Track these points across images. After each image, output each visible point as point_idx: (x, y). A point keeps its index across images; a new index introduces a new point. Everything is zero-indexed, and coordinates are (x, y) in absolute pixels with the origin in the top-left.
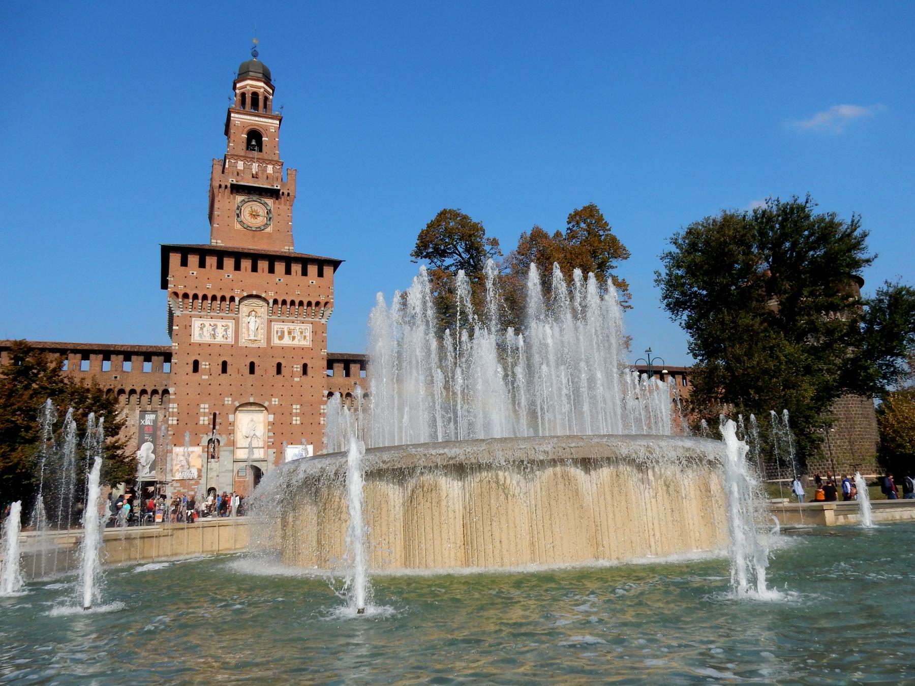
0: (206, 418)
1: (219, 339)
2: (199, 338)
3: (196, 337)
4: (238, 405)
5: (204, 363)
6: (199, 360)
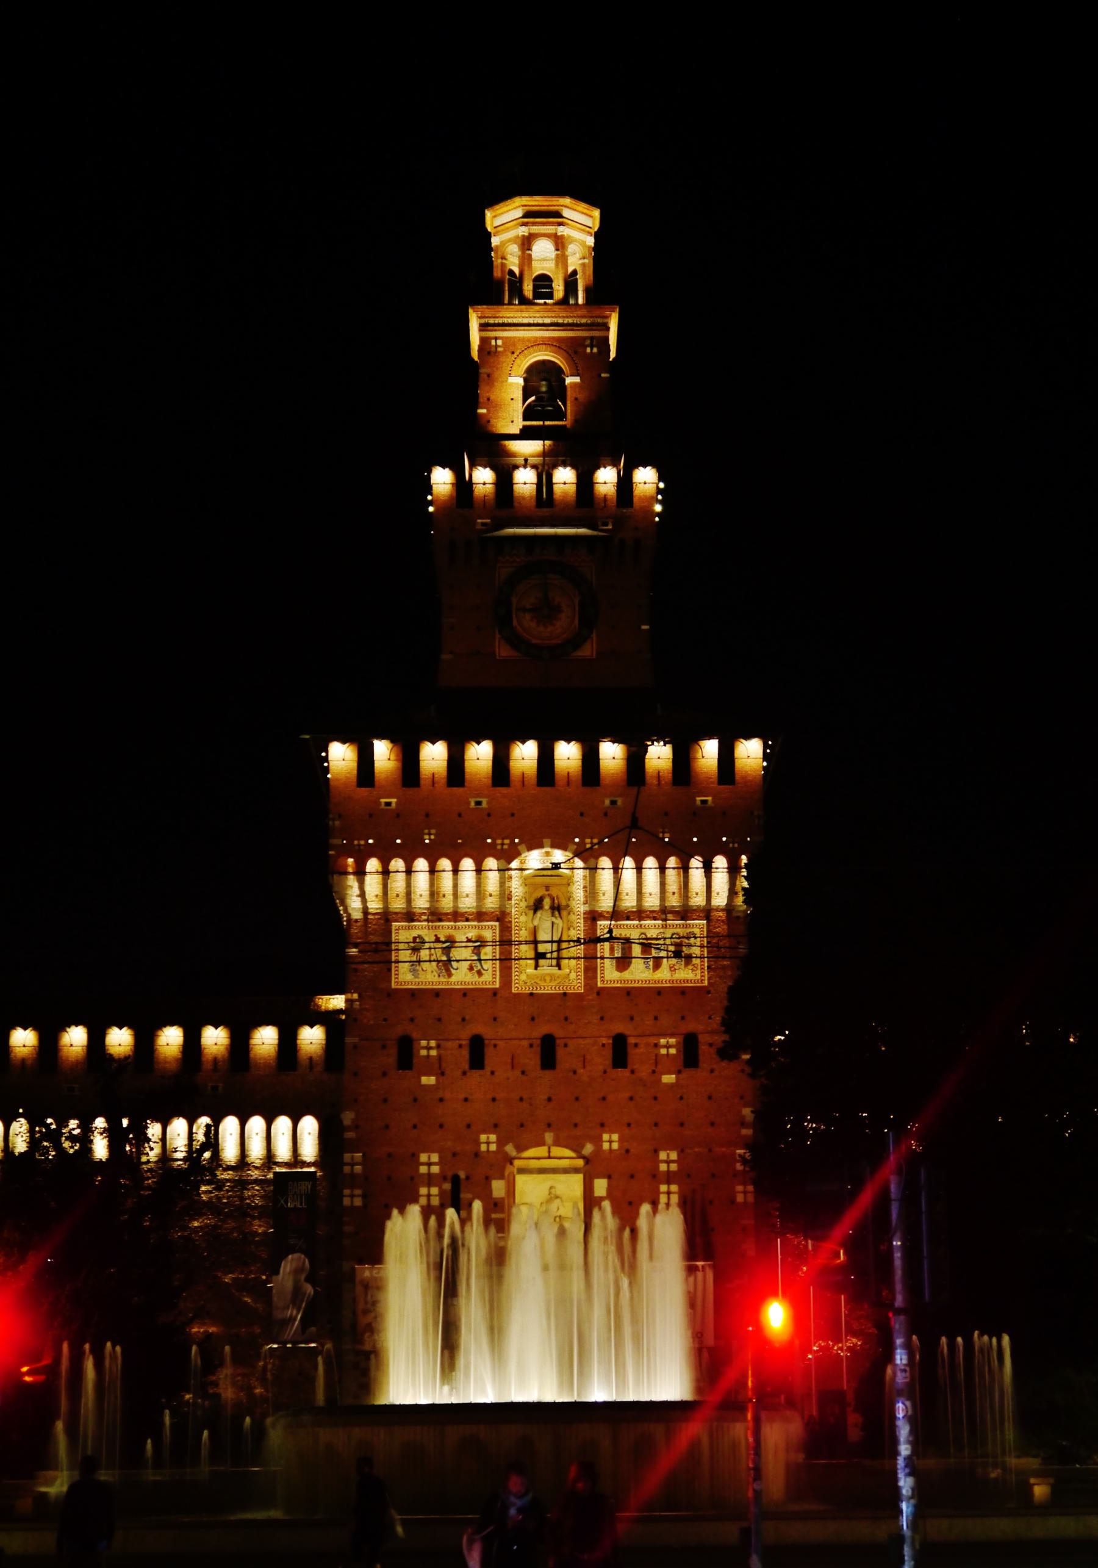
0: (435, 1191)
1: (461, 976)
2: (409, 977)
3: (404, 976)
5: (424, 1043)
6: (414, 1035)
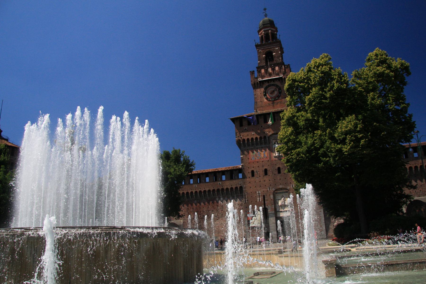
4: (274, 189)
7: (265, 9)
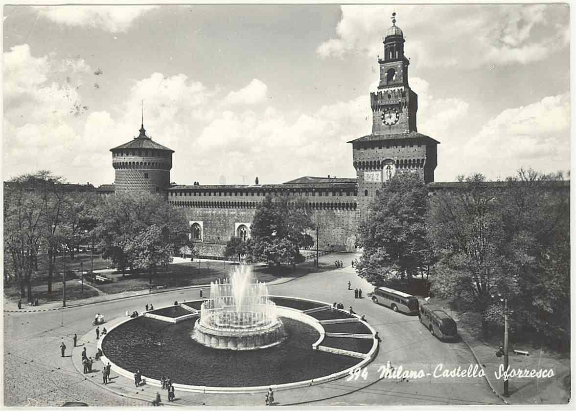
1: (375, 181)
7: (394, 14)
